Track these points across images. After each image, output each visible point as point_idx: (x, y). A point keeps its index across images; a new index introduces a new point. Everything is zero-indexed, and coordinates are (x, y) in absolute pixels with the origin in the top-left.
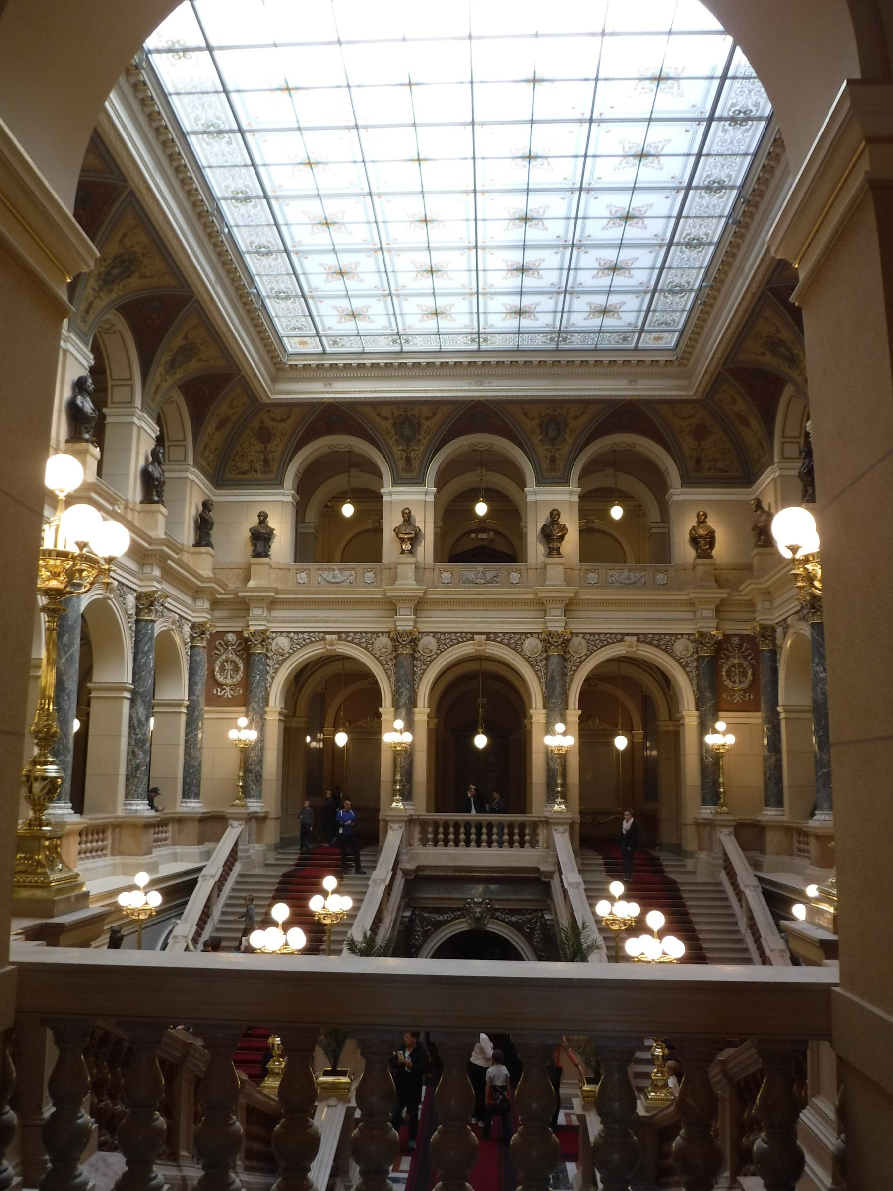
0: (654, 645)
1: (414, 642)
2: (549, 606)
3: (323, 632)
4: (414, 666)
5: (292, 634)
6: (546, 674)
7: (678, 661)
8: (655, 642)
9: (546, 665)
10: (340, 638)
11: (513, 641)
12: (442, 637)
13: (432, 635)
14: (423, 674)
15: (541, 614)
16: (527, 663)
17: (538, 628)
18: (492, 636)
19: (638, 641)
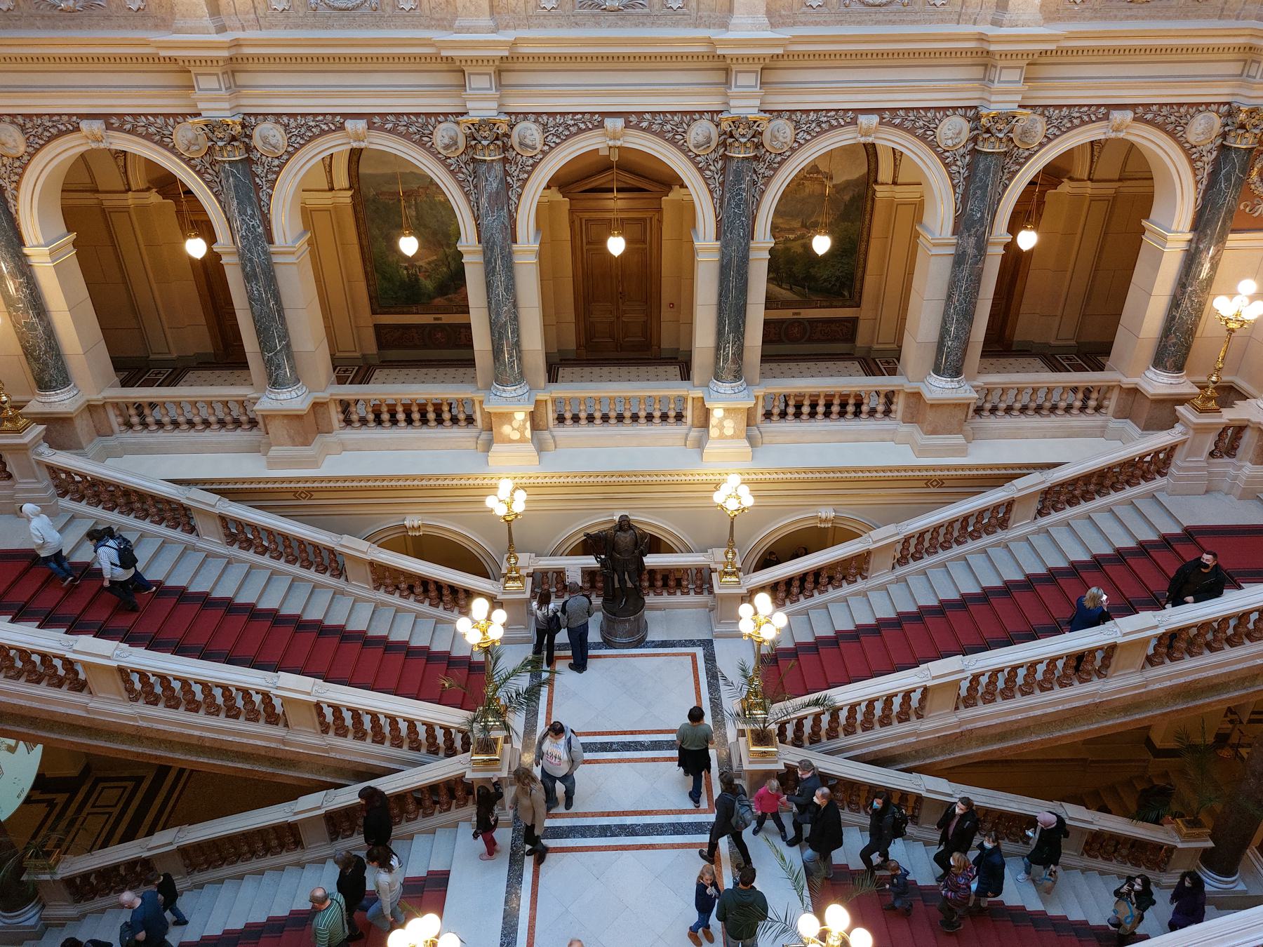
0: (907, 130)
1: (502, 141)
2: (735, 68)
3: (342, 115)
4: (506, 173)
5: (285, 119)
6: (722, 184)
7: (939, 155)
8: (907, 124)
9: (723, 169)
10: (371, 126)
11: (668, 127)
12: (551, 122)
13: (532, 118)
14: (522, 187)
15: (719, 77)
16: (690, 164)
17: (712, 103)
18: (633, 119)
19: (881, 123)
